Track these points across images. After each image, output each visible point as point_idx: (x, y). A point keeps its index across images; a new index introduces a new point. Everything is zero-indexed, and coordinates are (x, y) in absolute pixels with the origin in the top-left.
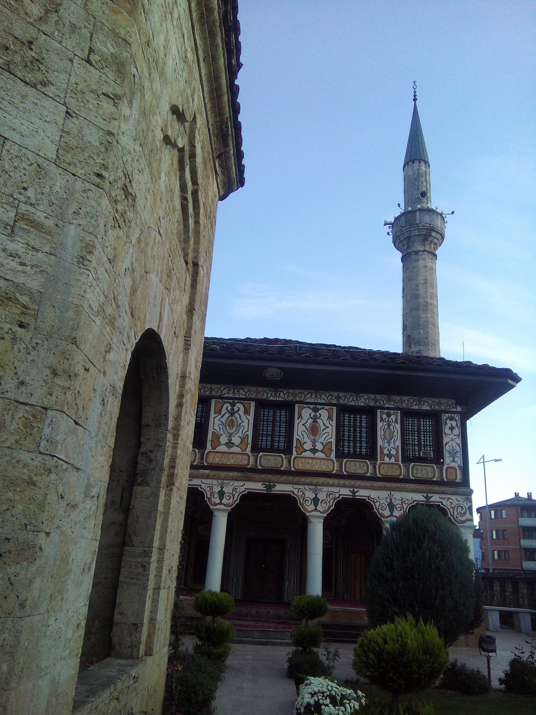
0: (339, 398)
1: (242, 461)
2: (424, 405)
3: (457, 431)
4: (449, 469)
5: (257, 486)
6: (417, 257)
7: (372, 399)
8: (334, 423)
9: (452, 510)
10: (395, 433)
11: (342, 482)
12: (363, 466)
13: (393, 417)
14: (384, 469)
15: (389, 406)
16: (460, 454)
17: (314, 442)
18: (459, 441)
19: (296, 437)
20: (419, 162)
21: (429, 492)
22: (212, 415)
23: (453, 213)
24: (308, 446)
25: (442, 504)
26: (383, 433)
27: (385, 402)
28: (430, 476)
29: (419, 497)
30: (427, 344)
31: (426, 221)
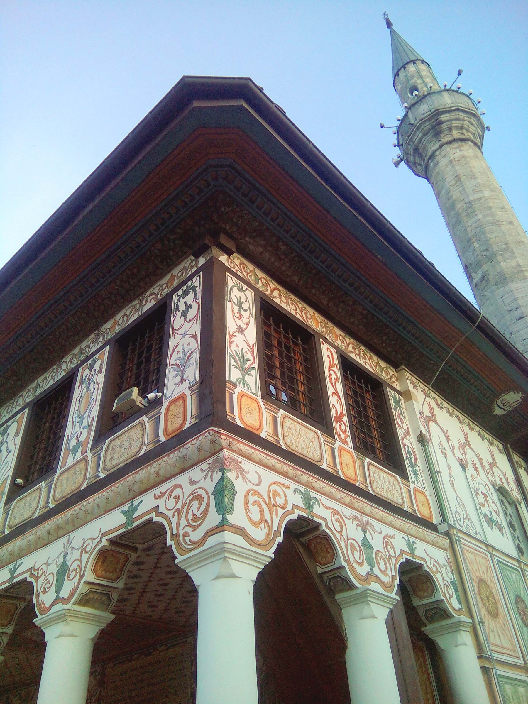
2: (147, 301)
3: (195, 310)
4: (172, 408)
6: (435, 161)
7: (76, 355)
8: (19, 440)
9: (174, 521)
10: (94, 396)
12: (35, 498)
14: (62, 483)
15: (97, 347)
18: (196, 328)
20: (405, 68)
23: (459, 74)
25: (159, 514)
26: (77, 408)
27: (92, 345)
29: (114, 521)
30: (491, 258)
31: (423, 112)
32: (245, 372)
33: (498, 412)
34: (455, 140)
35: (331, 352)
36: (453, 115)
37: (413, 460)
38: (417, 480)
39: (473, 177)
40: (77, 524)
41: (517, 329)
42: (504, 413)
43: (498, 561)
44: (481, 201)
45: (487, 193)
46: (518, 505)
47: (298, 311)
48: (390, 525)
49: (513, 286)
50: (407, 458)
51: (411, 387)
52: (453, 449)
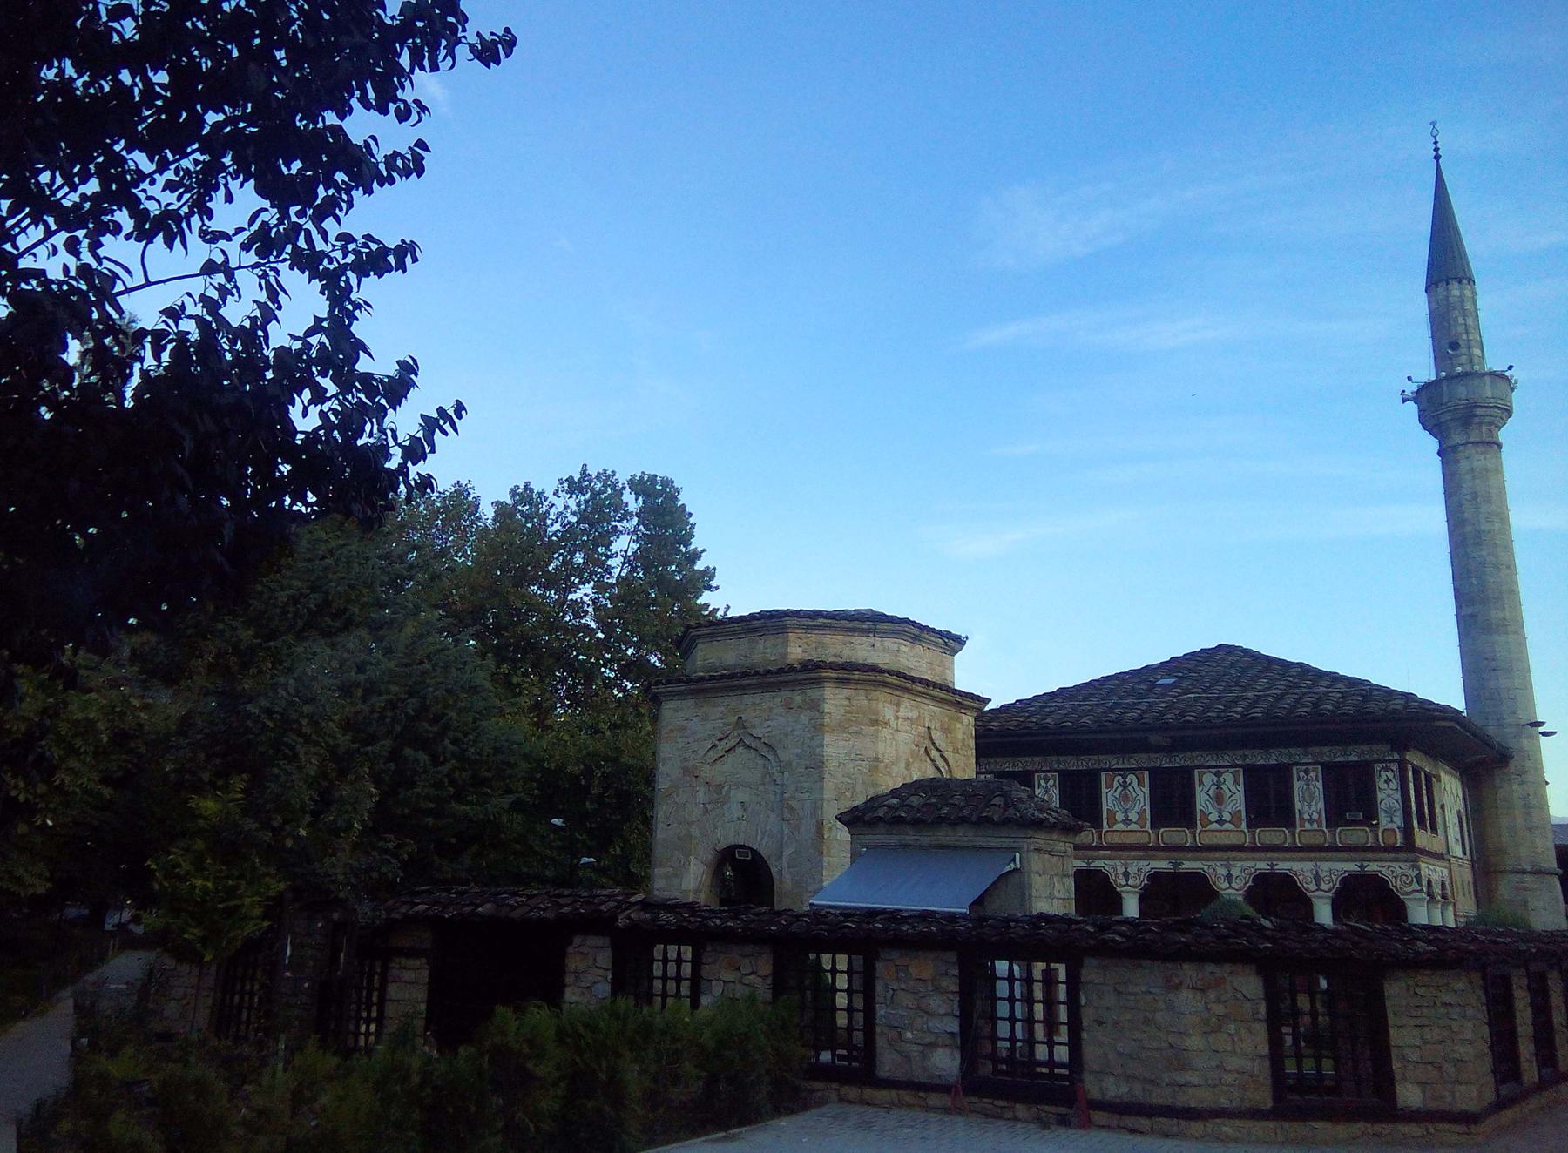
0: (1245, 756)
1: (1141, 839)
3: (1394, 785)
5: (1163, 865)
11: (1257, 855)
13: (1313, 774)
16: (1400, 813)
17: (1220, 813)
18: (1398, 796)
19: (1198, 807)
21: (1362, 860)
22: (1104, 790)
23: (1510, 368)
24: (1214, 817)
28: (1363, 841)
29: (1352, 867)
34: (1482, 442)
36: (1489, 411)
39: (1489, 501)
40: (1321, 860)
45: (1497, 526)
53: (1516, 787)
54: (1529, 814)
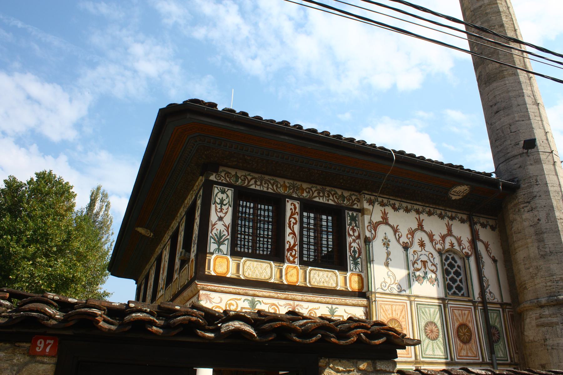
32: (219, 243)
33: (454, 198)
35: (295, 205)
37: (357, 256)
38: (356, 269)
41: (494, 121)
42: (461, 197)
43: (417, 304)
44: (482, 9)
46: (465, 258)
47: (270, 186)
48: (318, 302)
49: (495, 85)
50: (351, 256)
51: (366, 205)
52: (400, 237)
53: (526, 215)
54: (541, 240)
